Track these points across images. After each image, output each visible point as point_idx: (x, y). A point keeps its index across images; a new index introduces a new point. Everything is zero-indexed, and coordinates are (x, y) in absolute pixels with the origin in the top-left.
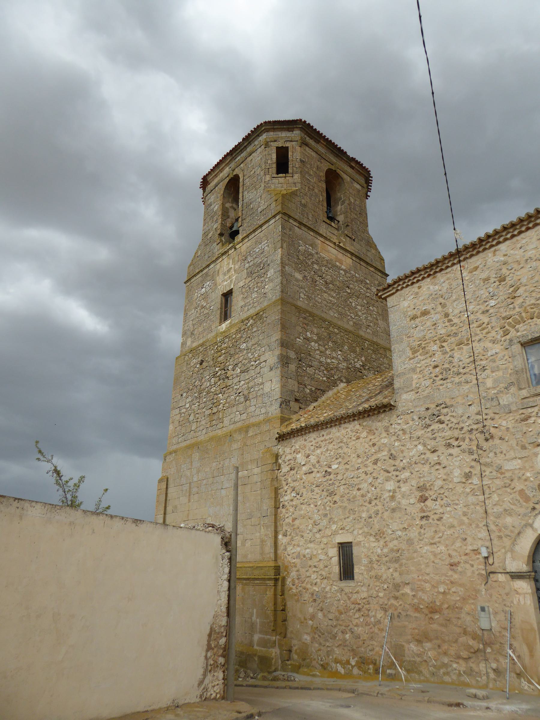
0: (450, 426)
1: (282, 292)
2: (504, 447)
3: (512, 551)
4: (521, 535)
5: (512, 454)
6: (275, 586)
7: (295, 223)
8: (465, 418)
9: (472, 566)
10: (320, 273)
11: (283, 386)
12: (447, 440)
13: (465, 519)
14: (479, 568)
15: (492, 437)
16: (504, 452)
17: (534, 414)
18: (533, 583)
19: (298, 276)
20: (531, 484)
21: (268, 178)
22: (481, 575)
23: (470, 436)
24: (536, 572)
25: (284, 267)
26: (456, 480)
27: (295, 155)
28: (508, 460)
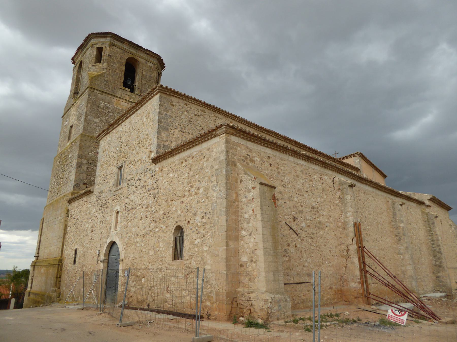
1: (84, 130)
6: (58, 267)
7: (98, 92)
10: (112, 117)
11: (76, 178)
19: (96, 120)
21: (90, 65)
25: (87, 117)
27: (106, 52)
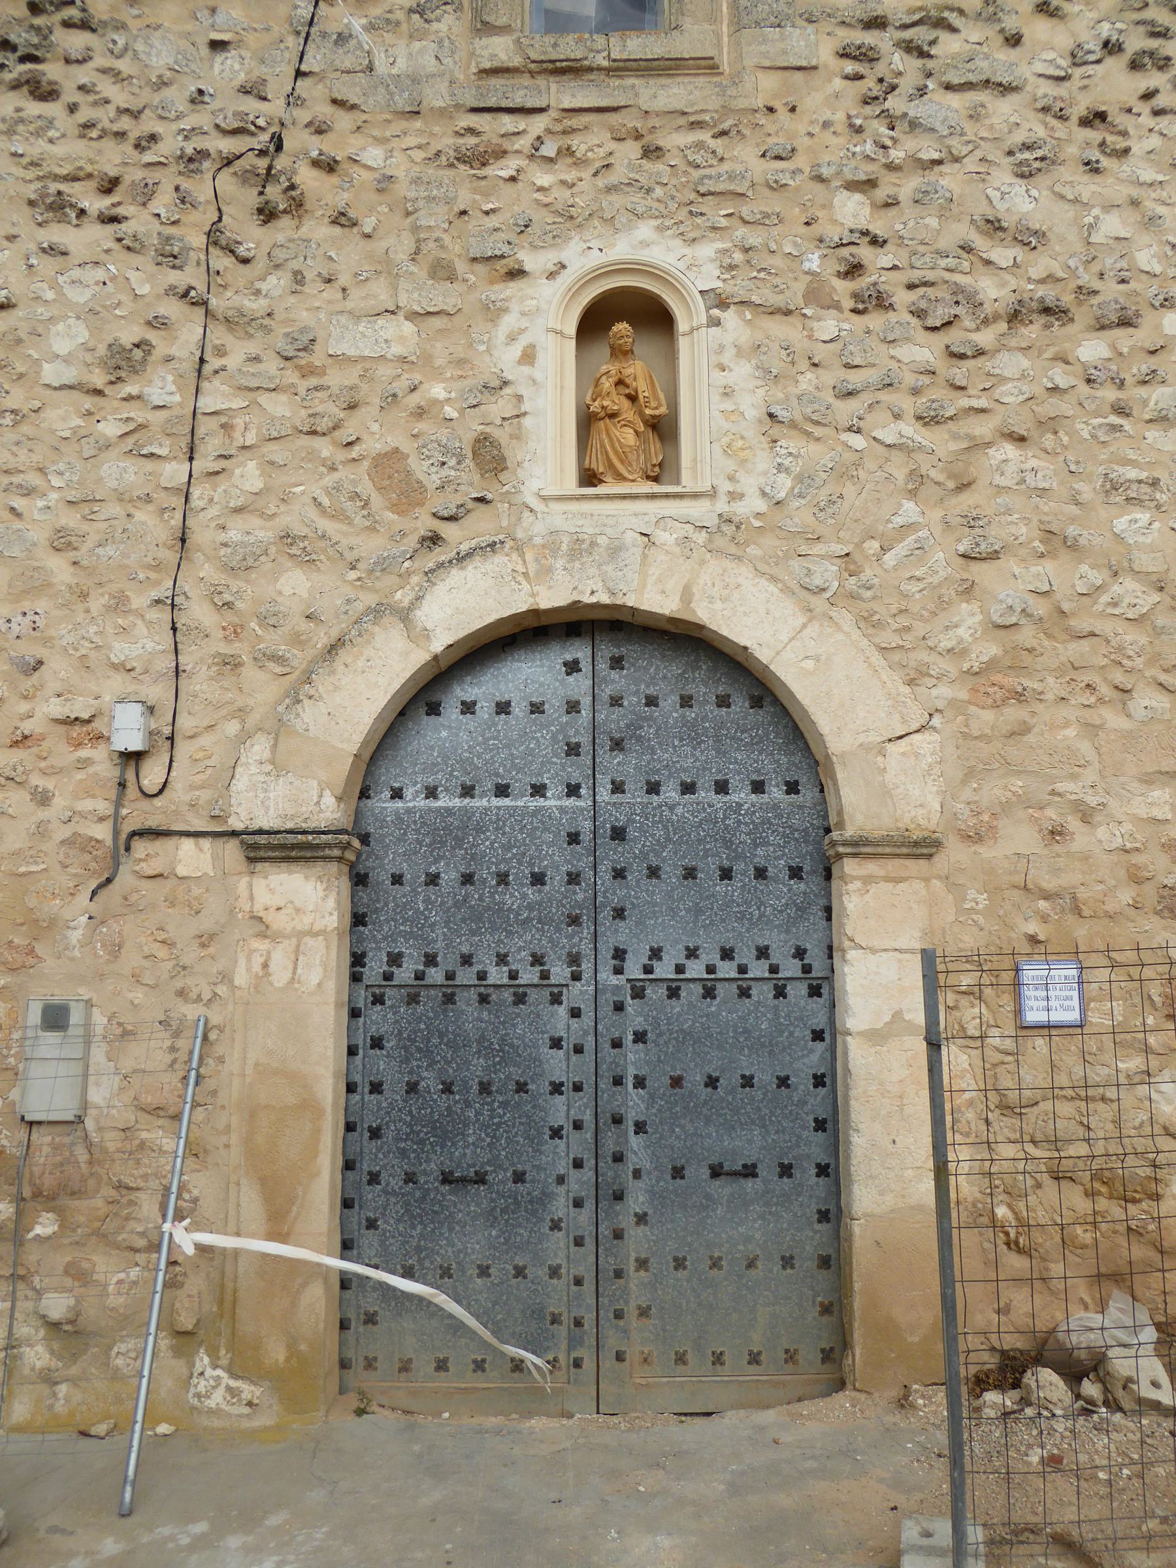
0: (82, 116)
2: (349, 255)
3: (279, 729)
4: (344, 655)
5: (380, 293)
8: (177, 96)
9: (43, 799)
12: (56, 178)
13: (59, 568)
14: (82, 802)
15: (297, 206)
16: (344, 280)
17: (524, 143)
18: (345, 884)
20: (443, 434)
22: (88, 844)
23: (185, 185)
24: (365, 839)
26: (51, 373)
28: (356, 316)
